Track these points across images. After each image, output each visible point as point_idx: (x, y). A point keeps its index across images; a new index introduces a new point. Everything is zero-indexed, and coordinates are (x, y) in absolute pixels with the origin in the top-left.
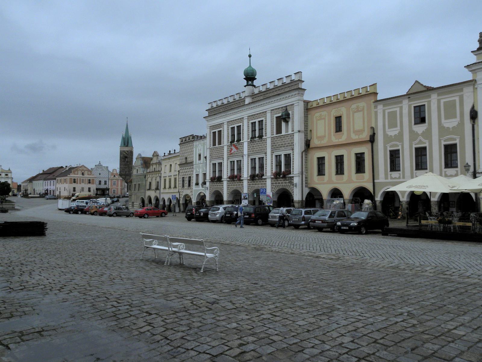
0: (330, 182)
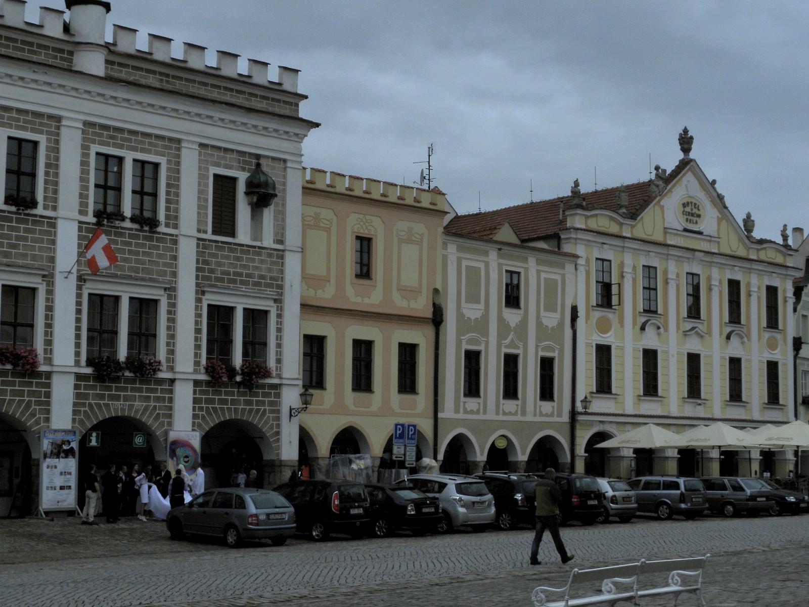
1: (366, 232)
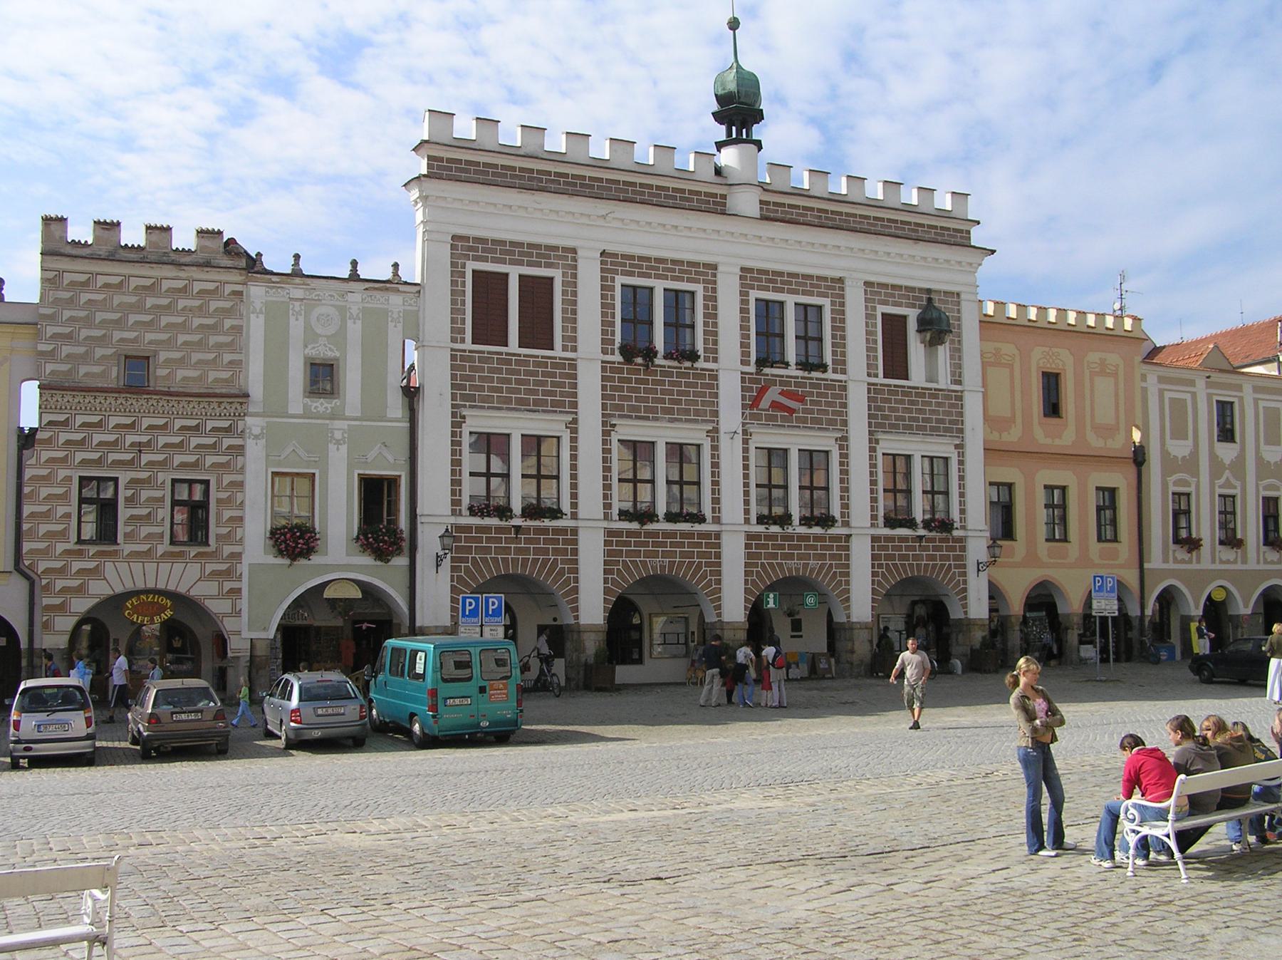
0: (1032, 559)
1: (1053, 366)
